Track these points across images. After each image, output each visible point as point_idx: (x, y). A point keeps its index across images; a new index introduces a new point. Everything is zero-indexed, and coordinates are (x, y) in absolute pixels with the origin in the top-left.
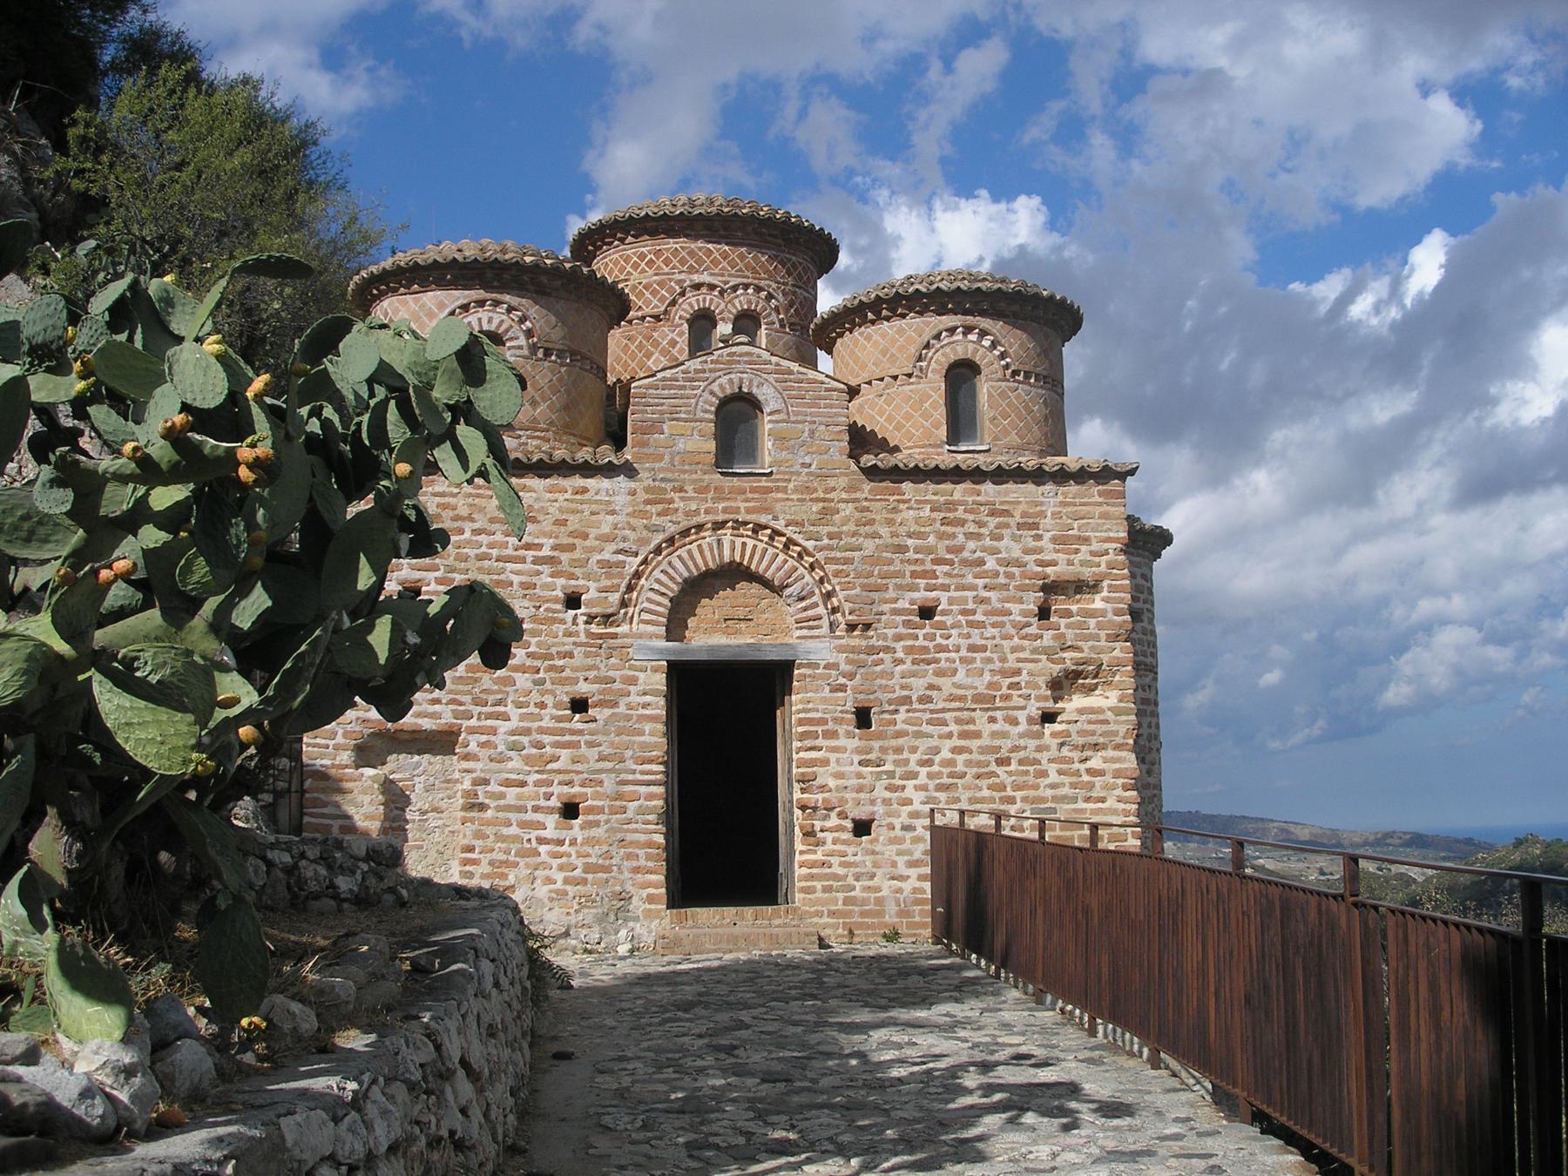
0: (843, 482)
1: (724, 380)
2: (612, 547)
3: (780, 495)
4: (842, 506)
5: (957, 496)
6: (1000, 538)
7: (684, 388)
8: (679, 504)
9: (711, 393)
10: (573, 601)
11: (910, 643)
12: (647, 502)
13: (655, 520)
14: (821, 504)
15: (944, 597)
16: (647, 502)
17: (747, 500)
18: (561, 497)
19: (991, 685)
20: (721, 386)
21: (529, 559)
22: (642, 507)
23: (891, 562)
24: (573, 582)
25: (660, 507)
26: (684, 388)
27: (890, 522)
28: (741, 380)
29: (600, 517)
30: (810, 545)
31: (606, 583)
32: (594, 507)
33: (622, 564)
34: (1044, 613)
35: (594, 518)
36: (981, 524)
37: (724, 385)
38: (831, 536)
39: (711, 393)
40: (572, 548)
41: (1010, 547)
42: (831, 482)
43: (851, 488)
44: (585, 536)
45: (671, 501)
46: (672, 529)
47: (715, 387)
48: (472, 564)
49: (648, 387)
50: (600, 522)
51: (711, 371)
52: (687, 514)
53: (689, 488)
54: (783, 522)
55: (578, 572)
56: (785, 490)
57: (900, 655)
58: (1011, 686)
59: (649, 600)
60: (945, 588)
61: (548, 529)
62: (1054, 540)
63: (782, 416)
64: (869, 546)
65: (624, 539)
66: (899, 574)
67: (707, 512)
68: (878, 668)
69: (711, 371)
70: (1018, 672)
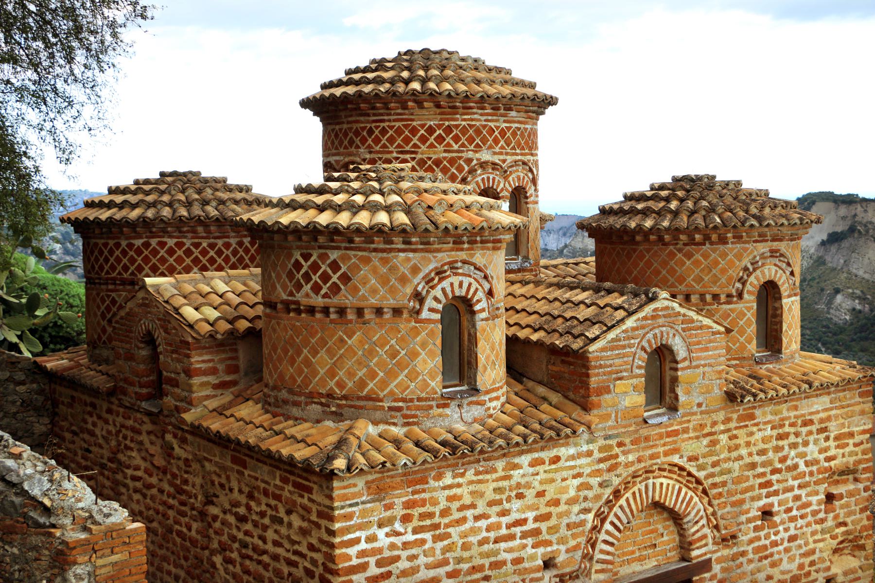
0: (721, 416)
1: (650, 336)
2: (576, 508)
3: (686, 436)
4: (722, 436)
5: (785, 414)
6: (806, 444)
7: (624, 347)
8: (622, 459)
9: (643, 349)
10: (548, 564)
11: (756, 544)
12: (601, 461)
13: (606, 477)
14: (709, 438)
15: (774, 500)
16: (601, 461)
17: (664, 445)
18: (540, 469)
19: (801, 567)
20: (649, 341)
21: (519, 535)
22: (597, 467)
23: (747, 479)
24: (549, 549)
25: (608, 464)
26: (624, 347)
27: (748, 444)
28: (662, 332)
29: (568, 482)
30: (701, 475)
31: (572, 543)
32: (565, 474)
33: (582, 523)
34: (830, 498)
35: (564, 484)
36: (797, 435)
37: (650, 340)
38: (714, 465)
39: (643, 349)
40: (546, 517)
41: (812, 451)
42: (714, 417)
43: (728, 420)
44: (556, 503)
45: (617, 456)
46: (616, 481)
47: (645, 344)
48: (475, 550)
49: (603, 349)
50: (567, 487)
51: (643, 327)
52: (627, 465)
53: (627, 441)
54: (685, 459)
55: (554, 538)
56: (686, 431)
57: (751, 556)
58: (812, 563)
59: (602, 551)
60: (776, 493)
61: (530, 503)
62: (836, 438)
63: (687, 363)
64: (736, 465)
65: (586, 499)
66: (751, 488)
67: (639, 460)
68: (739, 571)
69: (643, 327)
70: (813, 552)
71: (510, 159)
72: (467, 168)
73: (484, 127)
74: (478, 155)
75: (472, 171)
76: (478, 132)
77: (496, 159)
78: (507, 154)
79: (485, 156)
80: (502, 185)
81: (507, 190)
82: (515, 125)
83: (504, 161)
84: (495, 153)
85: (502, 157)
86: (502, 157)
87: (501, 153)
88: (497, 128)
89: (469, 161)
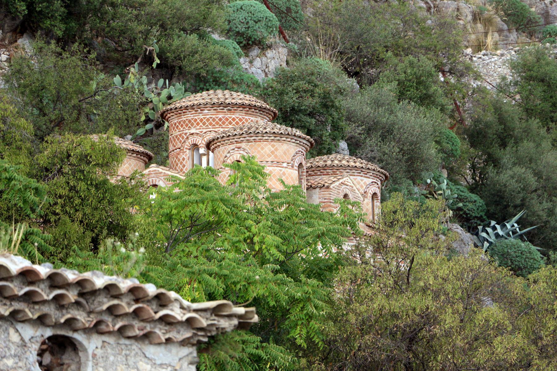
71: (204, 131)
72: (185, 137)
73: (192, 119)
74: (190, 131)
75: (187, 138)
76: (190, 121)
77: (198, 131)
78: (203, 129)
79: (193, 131)
80: (200, 142)
81: (203, 144)
82: (208, 117)
83: (201, 132)
84: (197, 129)
85: (200, 130)
86: (200, 130)
87: (200, 129)
88: (199, 118)
89: (186, 134)
